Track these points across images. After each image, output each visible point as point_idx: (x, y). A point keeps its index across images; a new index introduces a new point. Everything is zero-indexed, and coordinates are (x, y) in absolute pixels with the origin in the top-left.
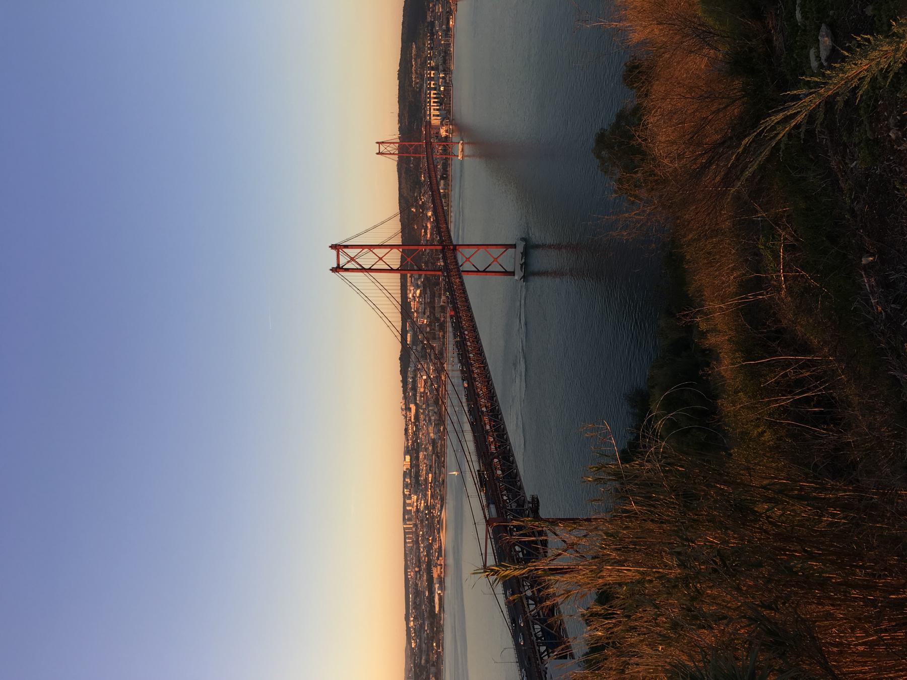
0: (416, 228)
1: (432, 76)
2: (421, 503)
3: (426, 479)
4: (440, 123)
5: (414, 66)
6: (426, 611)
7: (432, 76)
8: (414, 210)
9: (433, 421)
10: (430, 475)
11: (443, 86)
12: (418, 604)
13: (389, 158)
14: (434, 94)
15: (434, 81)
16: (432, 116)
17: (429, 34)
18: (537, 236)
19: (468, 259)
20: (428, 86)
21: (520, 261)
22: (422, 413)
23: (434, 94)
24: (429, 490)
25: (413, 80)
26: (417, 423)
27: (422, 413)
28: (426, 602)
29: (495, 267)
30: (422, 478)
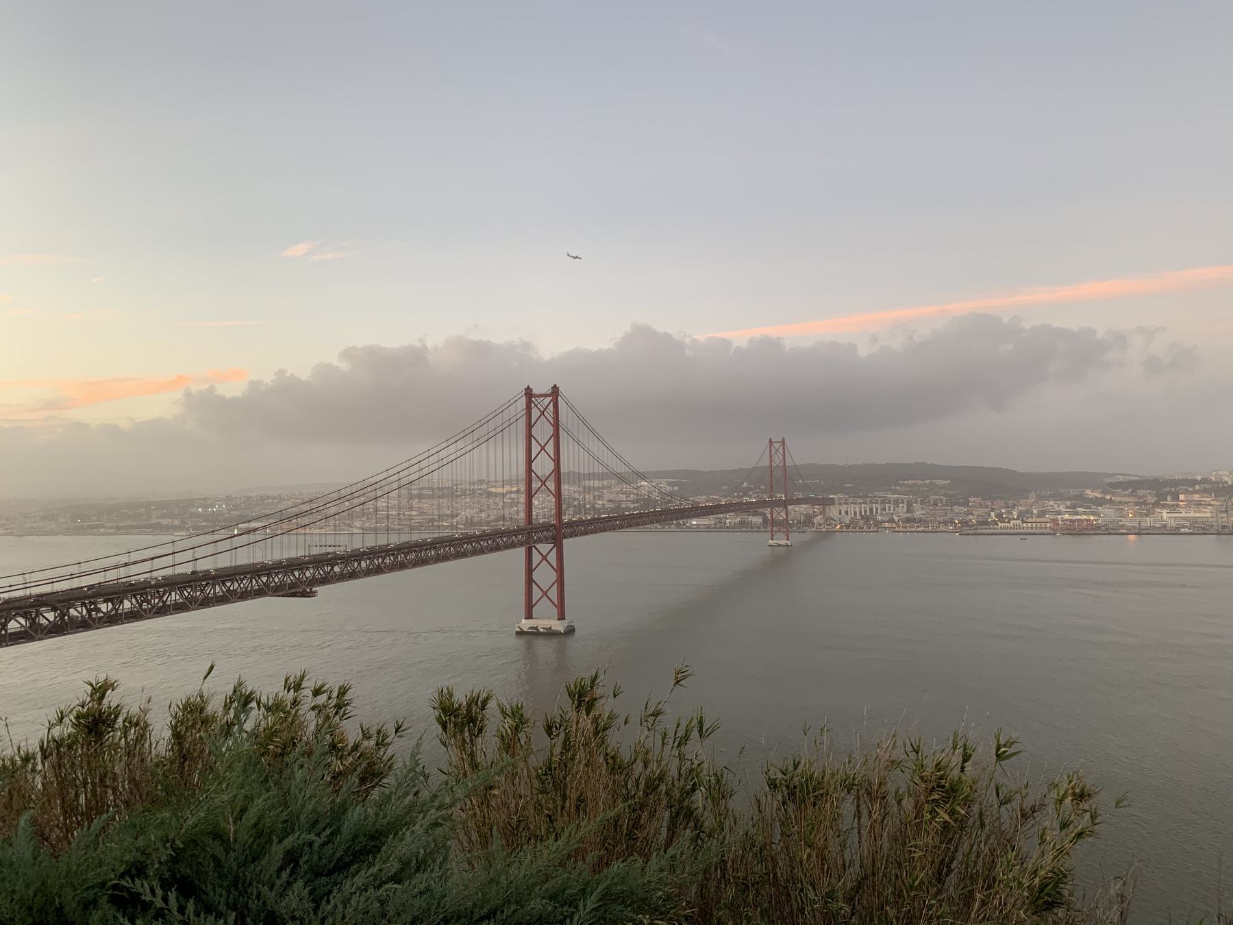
1: (901, 505)
4: (831, 515)
5: (923, 483)
6: (253, 512)
7: (901, 505)
8: (745, 484)
13: (762, 455)
14: (877, 509)
15: (894, 508)
16: (846, 506)
18: (574, 646)
19: (544, 558)
21: (541, 623)
23: (877, 509)
25: (906, 482)
29: (536, 593)
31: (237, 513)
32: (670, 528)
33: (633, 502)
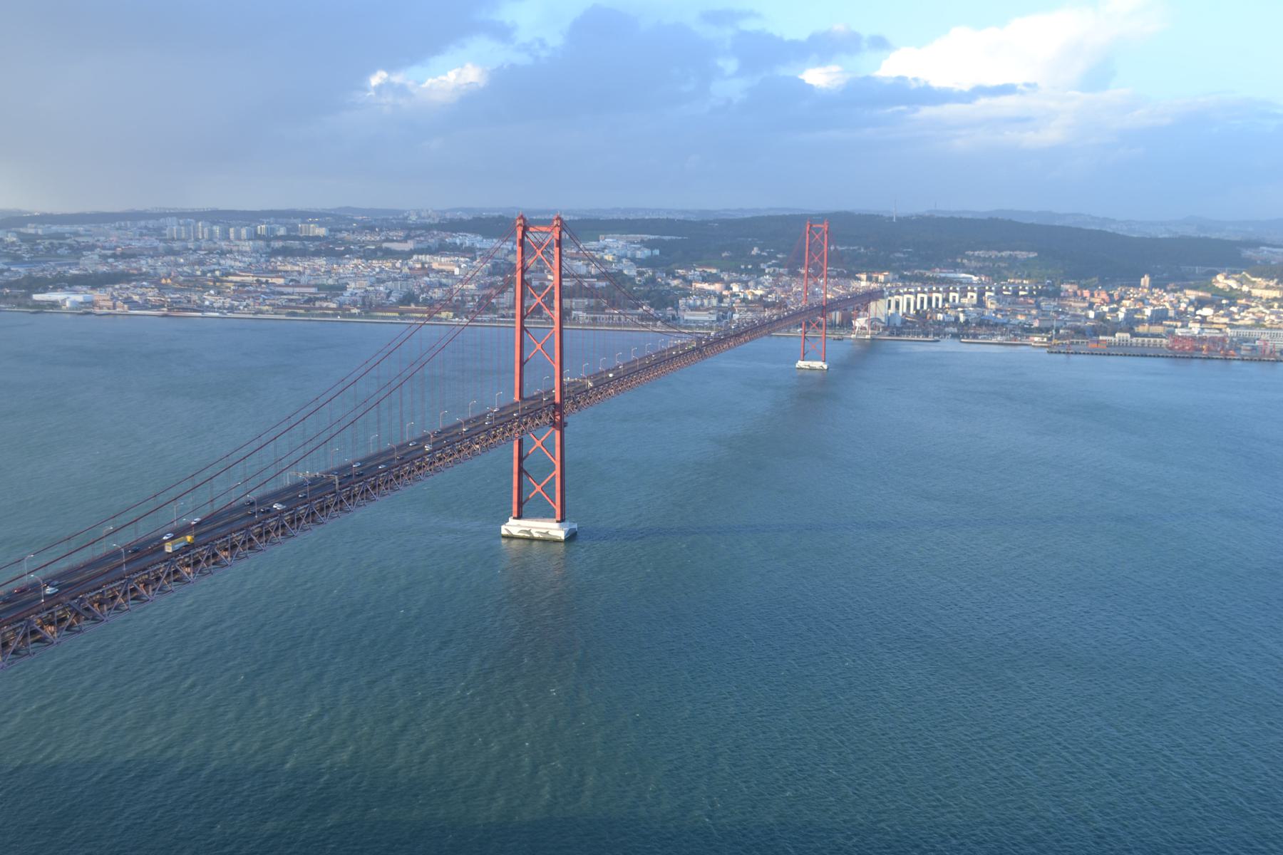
0: (724, 255)
2: (236, 260)
3: (275, 272)
6: (43, 270)
7: (969, 294)
9: (378, 288)
10: (281, 281)
11: (944, 318)
12: (59, 252)
15: (960, 298)
16: (896, 297)
17: (1040, 287)
20: (951, 288)
22: (394, 265)
24: (256, 278)
26: (379, 254)
27: (394, 265)
28: (59, 269)
30: (279, 263)
31: (22, 271)
32: (655, 326)
33: (598, 277)
